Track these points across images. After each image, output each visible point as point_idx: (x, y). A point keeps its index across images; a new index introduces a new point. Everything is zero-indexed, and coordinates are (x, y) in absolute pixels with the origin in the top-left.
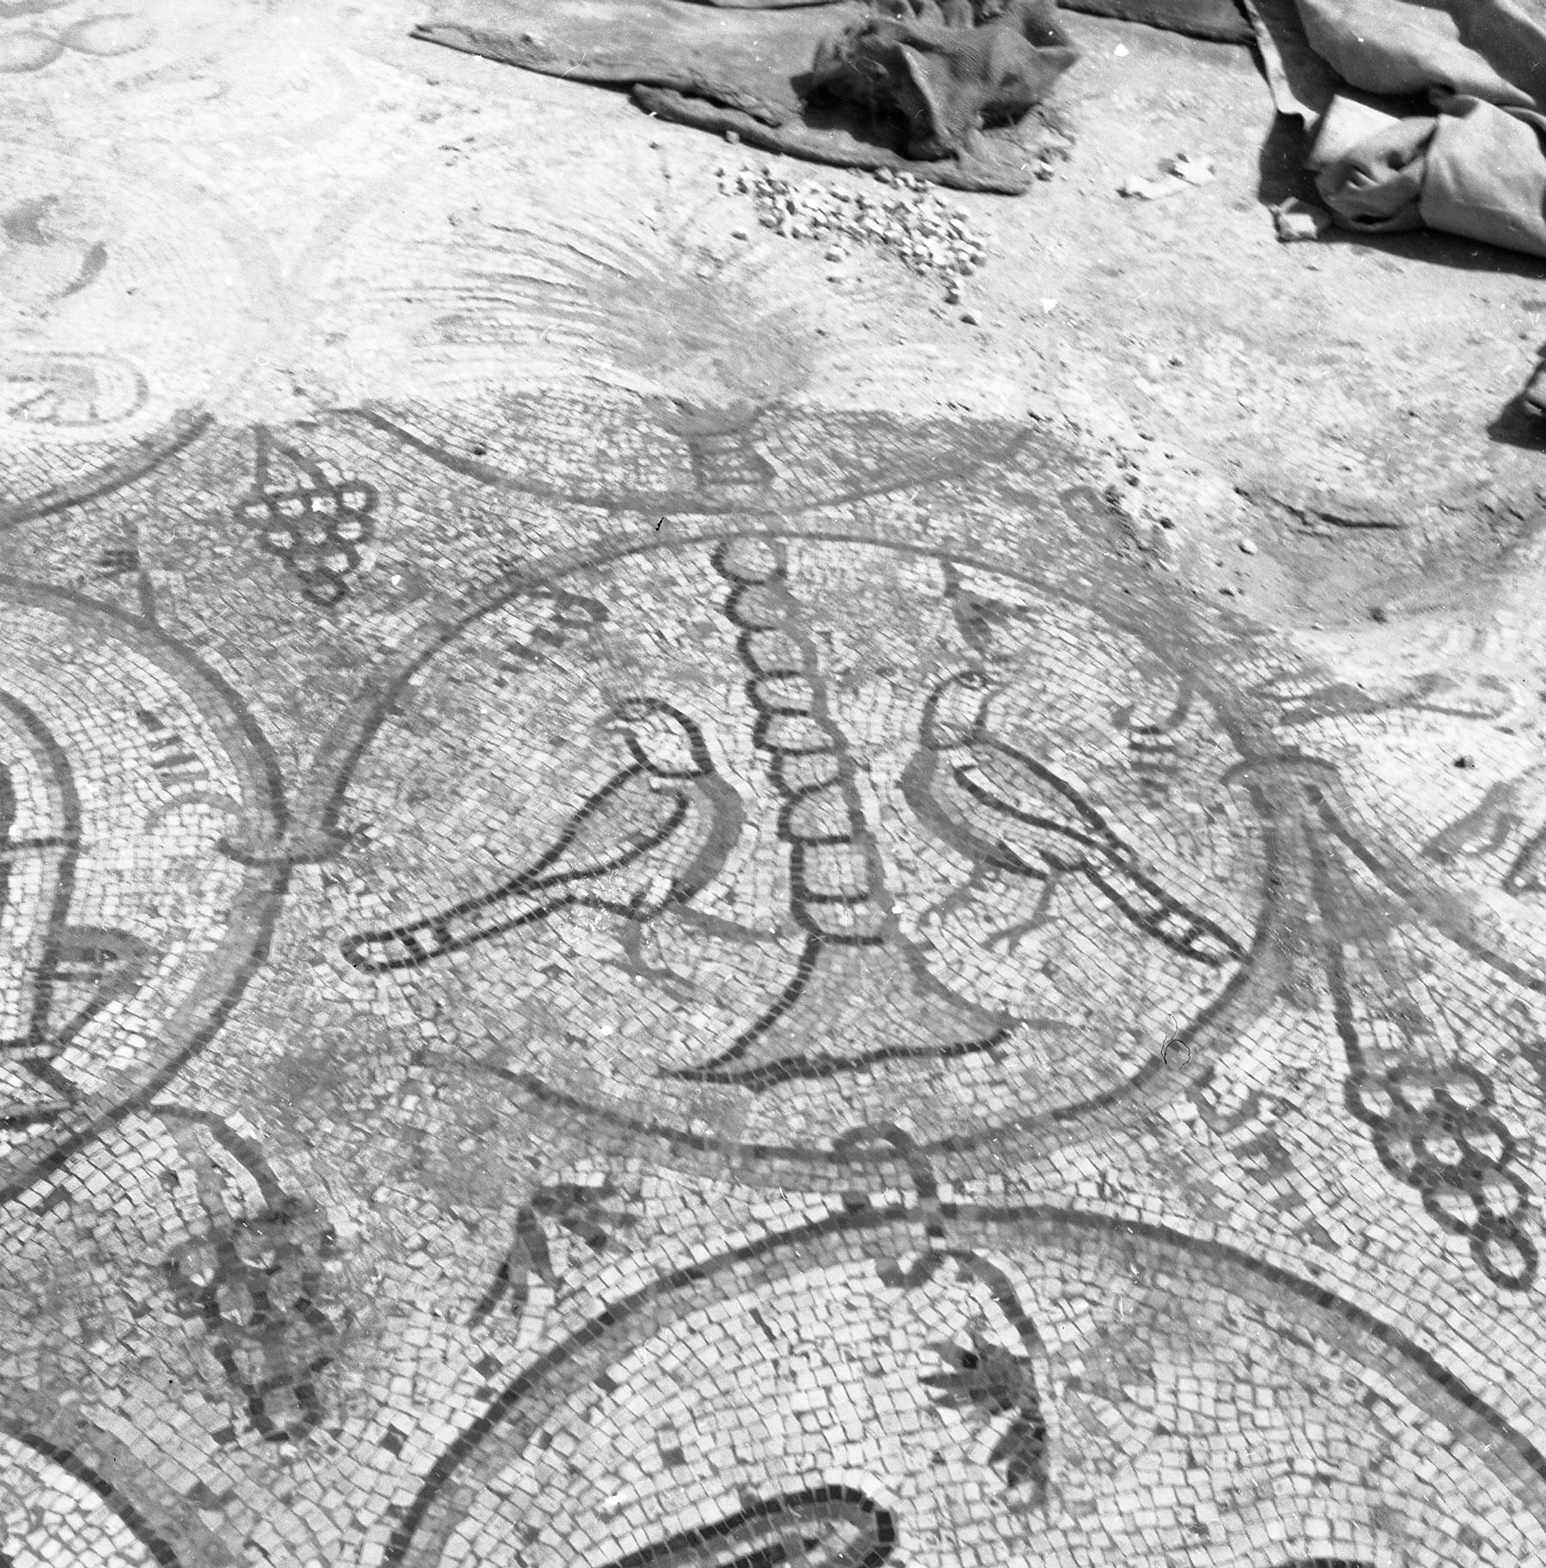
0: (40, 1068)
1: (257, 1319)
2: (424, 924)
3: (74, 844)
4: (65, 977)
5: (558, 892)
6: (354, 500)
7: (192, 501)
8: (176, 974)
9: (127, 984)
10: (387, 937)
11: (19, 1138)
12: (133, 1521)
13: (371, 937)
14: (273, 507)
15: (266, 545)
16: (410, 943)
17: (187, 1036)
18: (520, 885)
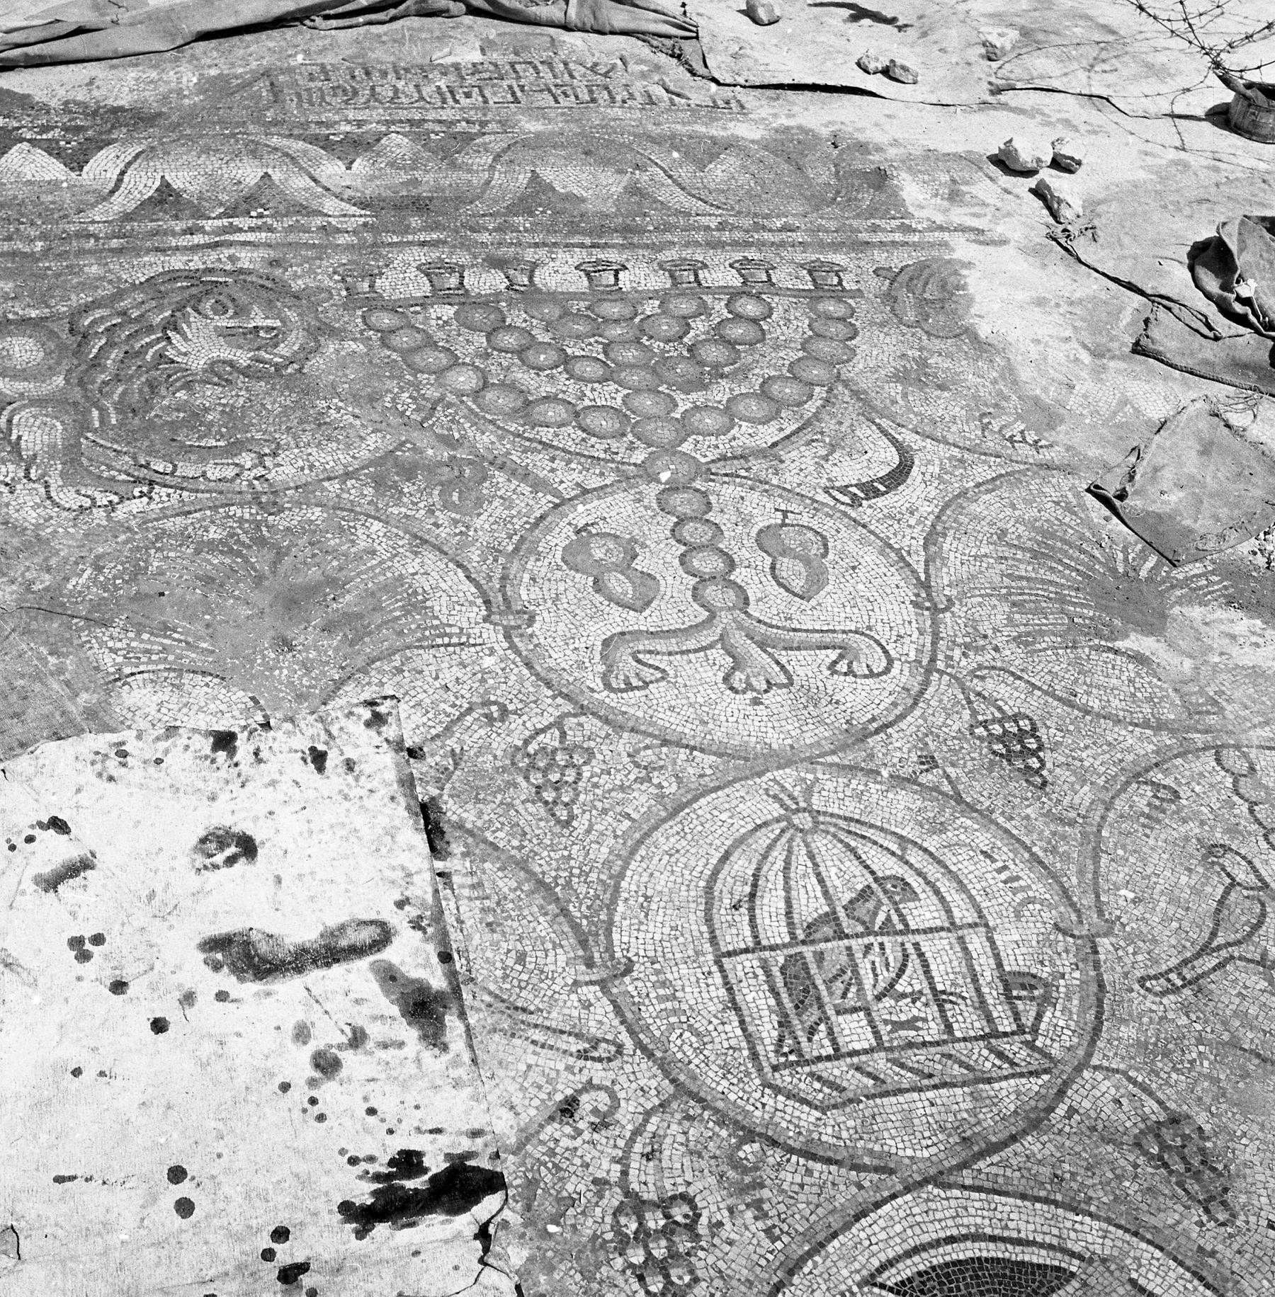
0: (1031, 1045)
1: (1188, 1170)
2: (1170, 970)
3: (987, 925)
4: (1019, 998)
5: (1224, 953)
6: (1025, 724)
7: (944, 724)
8: (1069, 998)
9: (1046, 1001)
10: (1156, 977)
11: (1040, 1082)
12: (1181, 1264)
13: (1150, 978)
14: (986, 728)
15: (994, 753)
16: (1169, 980)
17: (1089, 1028)
18: (1206, 949)
